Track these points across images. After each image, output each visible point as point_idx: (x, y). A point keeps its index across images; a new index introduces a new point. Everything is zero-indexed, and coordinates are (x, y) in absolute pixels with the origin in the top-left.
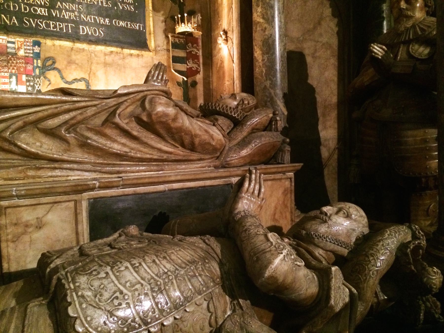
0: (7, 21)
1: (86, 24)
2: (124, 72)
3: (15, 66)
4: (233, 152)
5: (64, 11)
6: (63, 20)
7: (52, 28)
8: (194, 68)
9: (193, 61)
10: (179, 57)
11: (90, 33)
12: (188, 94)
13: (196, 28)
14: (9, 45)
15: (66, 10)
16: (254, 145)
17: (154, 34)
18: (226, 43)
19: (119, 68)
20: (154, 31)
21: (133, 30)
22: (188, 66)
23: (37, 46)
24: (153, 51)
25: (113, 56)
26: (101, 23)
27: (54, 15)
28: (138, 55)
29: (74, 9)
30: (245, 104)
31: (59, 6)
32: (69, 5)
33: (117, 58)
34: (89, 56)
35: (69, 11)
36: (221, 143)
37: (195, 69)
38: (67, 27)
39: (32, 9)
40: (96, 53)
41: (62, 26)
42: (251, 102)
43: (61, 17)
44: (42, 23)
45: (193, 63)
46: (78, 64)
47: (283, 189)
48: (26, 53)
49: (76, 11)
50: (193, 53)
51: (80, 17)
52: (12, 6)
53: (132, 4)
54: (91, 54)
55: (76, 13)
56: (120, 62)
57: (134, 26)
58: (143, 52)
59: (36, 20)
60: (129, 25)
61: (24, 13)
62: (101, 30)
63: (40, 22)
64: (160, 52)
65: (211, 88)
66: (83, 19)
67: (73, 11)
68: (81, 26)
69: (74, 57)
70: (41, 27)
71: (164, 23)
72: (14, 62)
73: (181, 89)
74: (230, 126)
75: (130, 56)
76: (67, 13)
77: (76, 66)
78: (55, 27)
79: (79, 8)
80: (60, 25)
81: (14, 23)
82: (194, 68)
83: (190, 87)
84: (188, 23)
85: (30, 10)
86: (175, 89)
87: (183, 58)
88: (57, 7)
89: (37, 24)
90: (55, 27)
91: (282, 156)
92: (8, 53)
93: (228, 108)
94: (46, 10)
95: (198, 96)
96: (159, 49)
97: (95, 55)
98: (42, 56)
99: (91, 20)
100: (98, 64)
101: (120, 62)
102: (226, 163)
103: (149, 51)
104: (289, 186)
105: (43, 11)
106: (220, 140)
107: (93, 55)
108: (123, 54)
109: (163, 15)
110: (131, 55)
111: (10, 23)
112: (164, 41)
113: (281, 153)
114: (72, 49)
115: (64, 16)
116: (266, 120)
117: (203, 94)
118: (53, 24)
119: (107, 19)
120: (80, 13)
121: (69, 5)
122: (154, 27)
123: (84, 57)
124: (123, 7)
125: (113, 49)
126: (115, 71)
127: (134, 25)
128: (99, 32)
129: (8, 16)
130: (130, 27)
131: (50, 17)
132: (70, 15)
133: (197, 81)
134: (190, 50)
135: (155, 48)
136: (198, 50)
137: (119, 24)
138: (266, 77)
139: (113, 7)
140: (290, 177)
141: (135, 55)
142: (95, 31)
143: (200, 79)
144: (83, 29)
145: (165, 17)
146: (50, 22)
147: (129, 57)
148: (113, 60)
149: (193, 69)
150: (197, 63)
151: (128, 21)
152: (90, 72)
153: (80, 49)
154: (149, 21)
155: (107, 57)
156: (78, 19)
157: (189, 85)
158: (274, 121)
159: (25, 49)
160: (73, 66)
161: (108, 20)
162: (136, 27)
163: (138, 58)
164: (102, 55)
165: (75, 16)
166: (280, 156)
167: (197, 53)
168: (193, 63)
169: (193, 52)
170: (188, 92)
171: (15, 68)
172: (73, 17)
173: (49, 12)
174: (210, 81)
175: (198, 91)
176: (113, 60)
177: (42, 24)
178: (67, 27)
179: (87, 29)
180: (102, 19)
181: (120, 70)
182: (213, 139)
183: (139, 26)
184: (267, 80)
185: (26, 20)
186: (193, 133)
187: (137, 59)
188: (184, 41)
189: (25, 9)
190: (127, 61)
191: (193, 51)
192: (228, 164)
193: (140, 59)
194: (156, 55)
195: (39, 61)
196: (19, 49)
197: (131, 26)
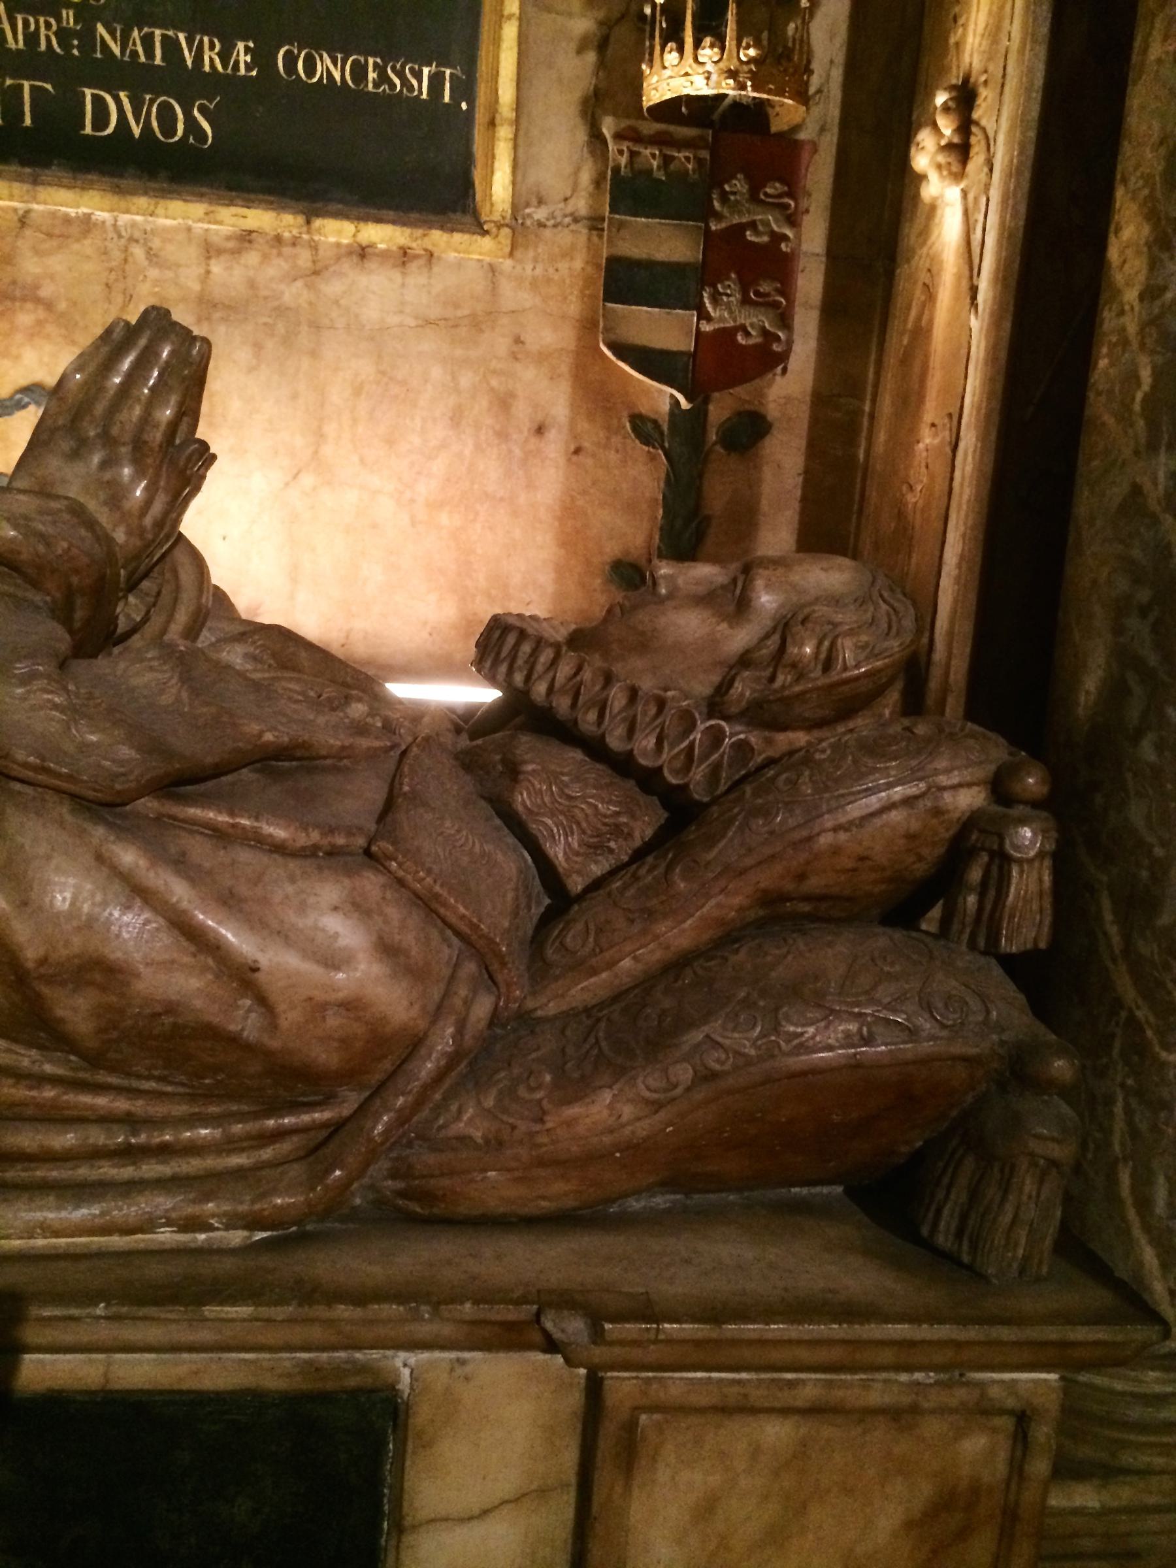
2: (314, 354)
4: (489, 1102)
8: (747, 334)
9: (745, 293)
10: (649, 265)
12: (699, 490)
13: (754, 77)
16: (684, 1073)
17: (517, 122)
18: (955, 168)
19: (281, 328)
20: (519, 105)
21: (394, 100)
22: (709, 319)
24: (499, 226)
25: (252, 258)
26: (207, 68)
28: (404, 256)
30: (794, 665)
33: (276, 267)
34: (117, 255)
36: (359, 1029)
37: (756, 339)
40: (156, 243)
42: (847, 652)
45: (745, 301)
46: (49, 306)
47: (926, 1489)
50: (749, 236)
54: (126, 250)
56: (293, 294)
57: (405, 82)
58: (437, 238)
60: (372, 75)
62: (202, 110)
64: (547, 233)
65: (861, 456)
68: (88, 92)
69: (30, 266)
71: (591, 57)
73: (653, 458)
74: (617, 831)
75: (355, 259)
77: (41, 313)
82: (747, 334)
83: (719, 449)
84: (697, 44)
86: (613, 457)
87: (676, 269)
91: (974, 1194)
93: (617, 698)
95: (765, 505)
96: (540, 214)
97: (152, 256)
99: (150, 54)
101: (293, 294)
102: (400, 1185)
103: (480, 229)
104: (1001, 1467)
106: (351, 1006)
107: (138, 252)
108: (314, 247)
110: (363, 253)
112: (577, 171)
113: (969, 1164)
114: (23, 221)
116: (911, 837)
117: (799, 493)
123: (89, 267)
125: (260, 218)
126: (258, 347)
127: (401, 75)
128: (190, 122)
130: (376, 85)
132: (32, 27)
133: (772, 411)
134: (736, 220)
135: (515, 207)
136: (792, 220)
137: (310, 69)
138: (1153, 426)
140: (1011, 1403)
141: (385, 255)
143: (788, 399)
144: (98, 102)
145: (601, 14)
147: (346, 266)
148: (252, 284)
149: (740, 338)
150: (775, 305)
151: (367, 54)
153: (67, 220)
154: (497, 41)
155: (217, 268)
156: (75, 52)
157: (713, 437)
158: (985, 858)
161: (247, 50)
162: (411, 88)
163: (404, 274)
164: (190, 254)
166: (959, 1195)
167: (785, 238)
168: (745, 301)
169: (757, 232)
170: (701, 476)
174: (859, 412)
175: (768, 473)
176: (252, 284)
180: (212, 47)
181: (287, 341)
182: (262, 1000)
183: (436, 81)
184: (1152, 447)
186: (31, 954)
187: (396, 275)
188: (700, 161)
190: (332, 288)
191: (753, 225)
192: (426, 1197)
193: (416, 277)
194: (518, 254)
197: (383, 78)
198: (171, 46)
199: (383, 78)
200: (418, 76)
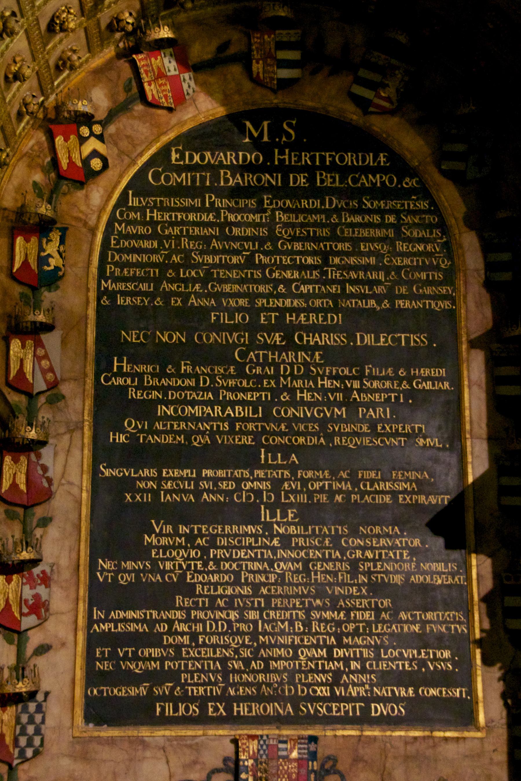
0: (280, 710)
1: (379, 700)
3: (286, 773)
5: (350, 686)
6: (349, 699)
7: (334, 712)
11: (385, 713)
14: (281, 746)
15: (354, 684)
17: (484, 702)
20: (484, 697)
23: (313, 743)
26: (402, 696)
27: (338, 693)
29: (365, 681)
31: (345, 681)
32: (358, 677)
35: (358, 685)
38: (354, 708)
39: (310, 690)
41: (347, 708)
43: (347, 695)
44: (322, 707)
48: (299, 753)
49: (367, 683)
51: (372, 691)
52: (287, 691)
53: (448, 660)
55: (367, 687)
59: (315, 704)
60: (444, 693)
61: (301, 696)
62: (402, 706)
63: (320, 706)
66: (376, 693)
67: (363, 684)
68: (373, 705)
70: (320, 712)
71: (502, 683)
72: (286, 768)
75: (444, 741)
76: (355, 688)
77: (365, 764)
78: (339, 710)
79: (371, 679)
80: (345, 707)
81: (289, 713)
85: (308, 691)
88: (342, 682)
89: (316, 710)
90: (339, 710)
92: (279, 757)
94: (328, 688)
97: (392, 746)
98: (319, 755)
100: (395, 758)
101: (429, 752)
105: (324, 690)
107: (388, 745)
109: (500, 669)
110: (446, 739)
111: (284, 712)
112: (501, 713)
115: (350, 693)
118: (336, 706)
119: (410, 689)
120: (371, 685)
121: (358, 677)
122: (484, 690)
124: (435, 667)
128: (399, 710)
129: (282, 703)
131: (333, 698)
137: (428, 693)
139: (420, 668)
142: (393, 709)
144: (376, 708)
146: (332, 705)
147: (442, 743)
148: (418, 751)
151: (442, 687)
152: (384, 771)
155: (409, 748)
159: (300, 749)
160: (360, 765)
164: (401, 745)
165: (366, 691)
171: (286, 776)
172: (363, 693)
173: (332, 691)
176: (418, 751)
177: (322, 709)
178: (354, 708)
179: (380, 707)
183: (461, 692)
185: (303, 706)
189: (303, 691)
190: (440, 749)
195: (315, 763)
196: (291, 751)
197: (447, 693)
198: (393, 691)
199: (447, 693)
200: (456, 691)
